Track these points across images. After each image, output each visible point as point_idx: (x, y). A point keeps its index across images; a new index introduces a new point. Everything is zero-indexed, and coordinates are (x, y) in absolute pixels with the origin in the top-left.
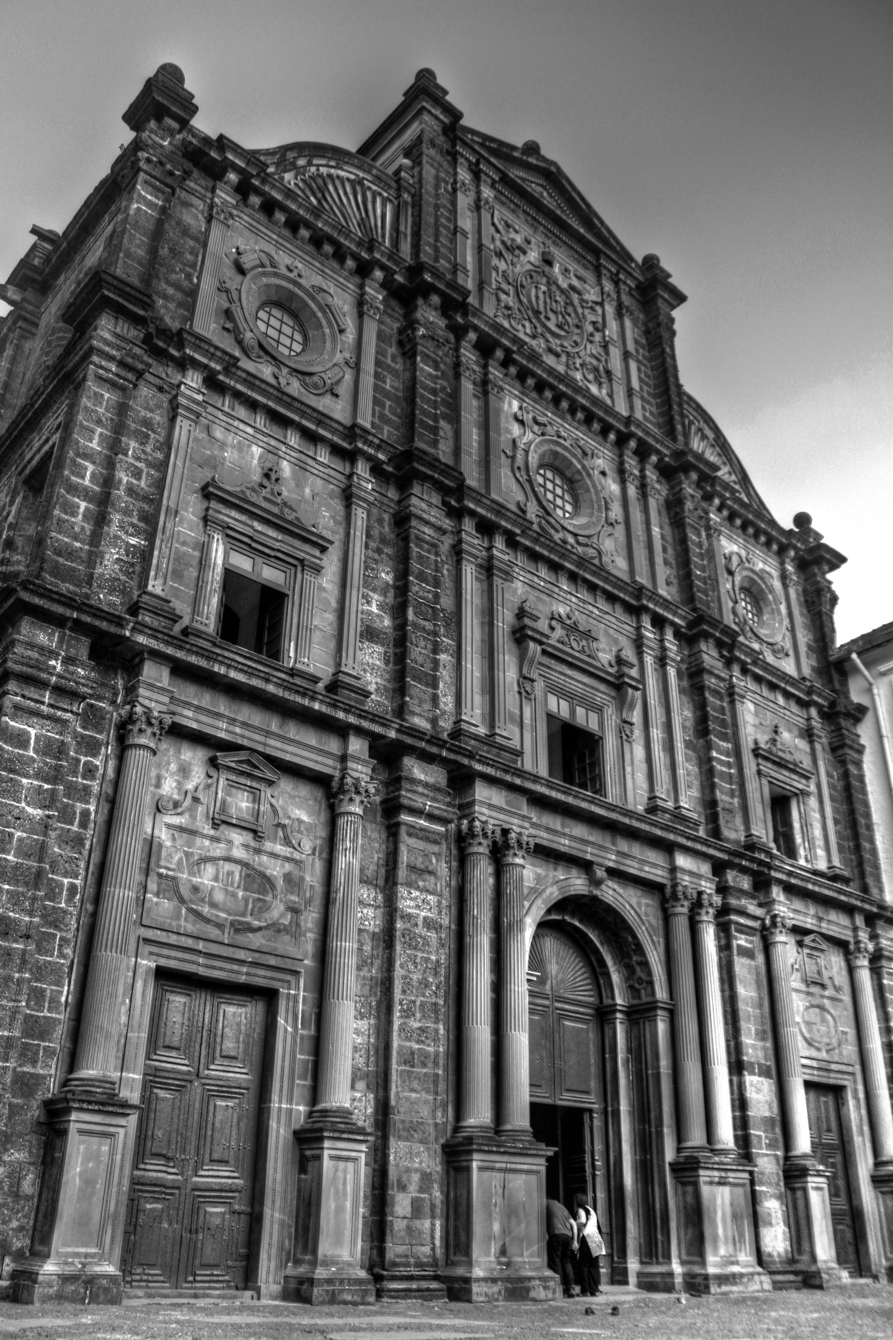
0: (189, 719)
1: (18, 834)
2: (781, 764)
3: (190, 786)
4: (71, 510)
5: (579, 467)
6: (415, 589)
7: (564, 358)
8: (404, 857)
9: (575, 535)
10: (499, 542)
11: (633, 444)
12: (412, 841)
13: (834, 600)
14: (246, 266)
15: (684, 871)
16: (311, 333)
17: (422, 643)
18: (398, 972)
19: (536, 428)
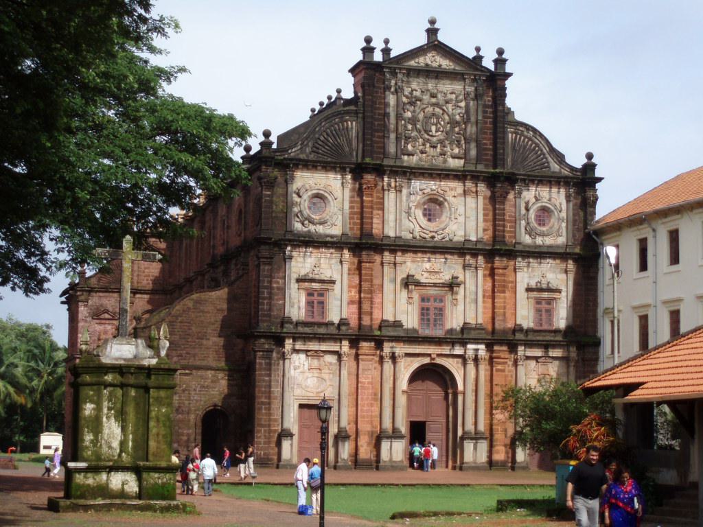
0: (298, 347)
1: (264, 384)
2: (541, 290)
3: (302, 362)
4: (263, 304)
5: (441, 199)
6: (363, 286)
7: (439, 145)
8: (361, 367)
9: (436, 232)
10: (399, 254)
11: (469, 177)
12: (363, 362)
13: (597, 199)
14: (301, 195)
15: (469, 349)
16: (326, 201)
17: (367, 302)
18: (359, 397)
19: (420, 193)
